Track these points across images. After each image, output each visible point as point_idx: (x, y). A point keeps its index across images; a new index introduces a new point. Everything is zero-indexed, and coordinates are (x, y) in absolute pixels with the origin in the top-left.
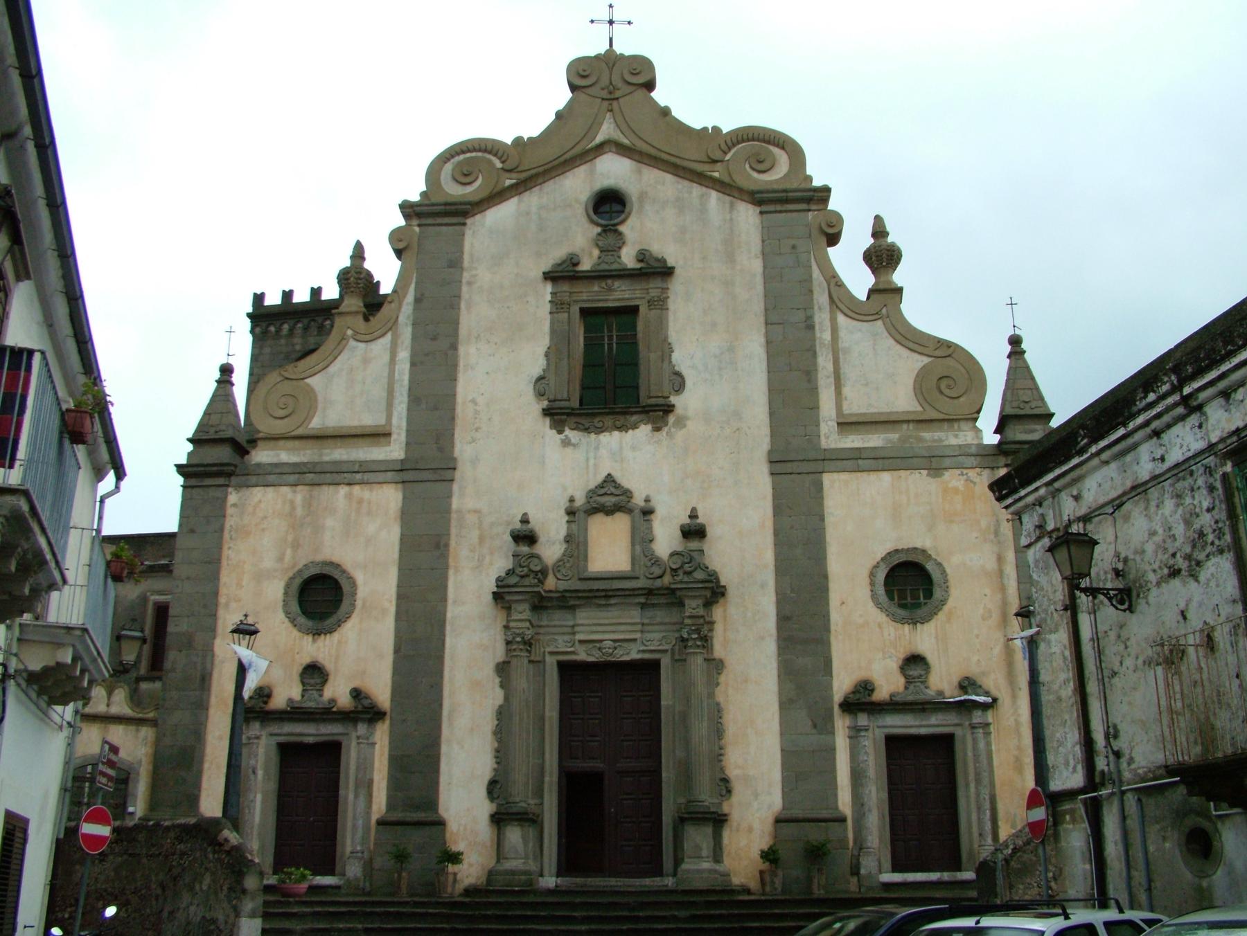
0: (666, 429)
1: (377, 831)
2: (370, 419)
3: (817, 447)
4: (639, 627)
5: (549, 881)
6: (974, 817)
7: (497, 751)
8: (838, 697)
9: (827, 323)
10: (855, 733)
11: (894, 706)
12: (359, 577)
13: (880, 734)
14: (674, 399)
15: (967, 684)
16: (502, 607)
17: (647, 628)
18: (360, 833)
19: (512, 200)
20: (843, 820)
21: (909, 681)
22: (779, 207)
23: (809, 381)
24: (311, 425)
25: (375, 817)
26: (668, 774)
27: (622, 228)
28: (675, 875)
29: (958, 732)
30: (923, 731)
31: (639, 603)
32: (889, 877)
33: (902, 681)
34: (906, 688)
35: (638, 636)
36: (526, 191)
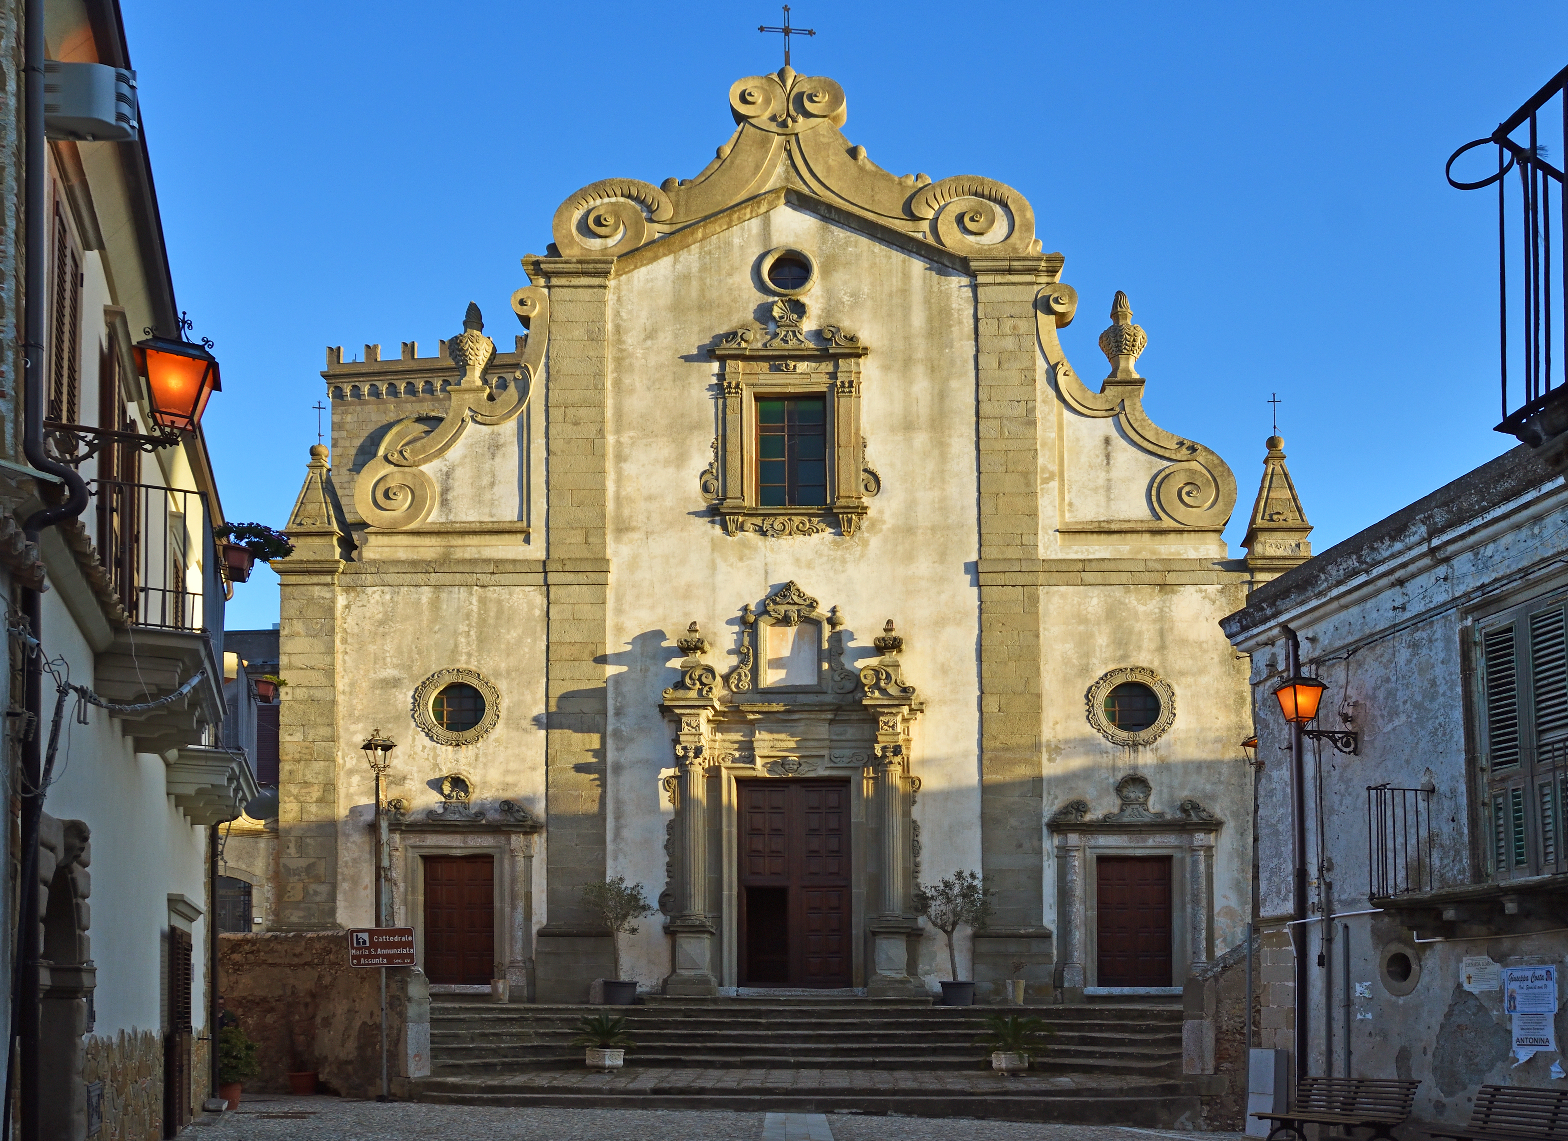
0: (858, 534)
1: (538, 942)
2: (509, 512)
3: (1034, 560)
4: (827, 743)
5: (731, 990)
6: (1189, 937)
7: (669, 865)
8: (1045, 820)
9: (1053, 418)
10: (1063, 854)
11: (1106, 826)
12: (502, 685)
13: (1092, 855)
14: (866, 500)
15: (1189, 807)
16: (670, 721)
17: (834, 744)
18: (518, 947)
19: (665, 259)
20: (1048, 936)
21: (1126, 803)
22: (999, 279)
23: (1028, 484)
24: (429, 520)
25: (535, 929)
26: (859, 889)
27: (803, 299)
28: (865, 985)
29: (1177, 855)
30: (1139, 853)
31: (824, 720)
32: (1093, 990)
33: (1118, 802)
34: (1122, 810)
35: (825, 752)
36: (682, 249)
